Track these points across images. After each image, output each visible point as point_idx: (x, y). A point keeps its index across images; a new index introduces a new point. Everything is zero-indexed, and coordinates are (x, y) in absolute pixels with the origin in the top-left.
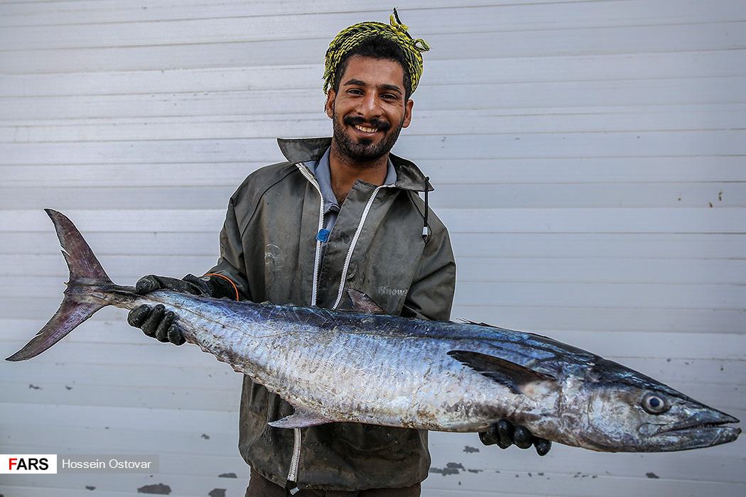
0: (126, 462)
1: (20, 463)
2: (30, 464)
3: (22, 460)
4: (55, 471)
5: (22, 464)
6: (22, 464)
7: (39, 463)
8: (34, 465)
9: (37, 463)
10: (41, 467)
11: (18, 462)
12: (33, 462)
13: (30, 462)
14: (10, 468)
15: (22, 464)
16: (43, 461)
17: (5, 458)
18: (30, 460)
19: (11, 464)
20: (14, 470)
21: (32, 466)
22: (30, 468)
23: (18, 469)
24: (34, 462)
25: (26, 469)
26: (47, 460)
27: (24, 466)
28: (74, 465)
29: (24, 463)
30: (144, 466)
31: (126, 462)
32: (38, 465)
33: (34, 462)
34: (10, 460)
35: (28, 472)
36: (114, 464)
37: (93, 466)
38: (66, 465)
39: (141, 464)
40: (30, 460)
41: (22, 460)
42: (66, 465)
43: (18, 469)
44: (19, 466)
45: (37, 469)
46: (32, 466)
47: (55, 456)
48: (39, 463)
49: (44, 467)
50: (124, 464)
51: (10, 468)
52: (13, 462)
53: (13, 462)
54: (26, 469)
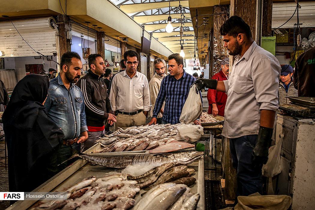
0: (53, 195)
1: (9, 196)
2: (13, 196)
3: (9, 194)
4: (23, 199)
5: (9, 196)
6: (9, 196)
7: (16, 195)
8: (14, 196)
9: (15, 196)
10: (17, 198)
11: (7, 195)
12: (14, 195)
13: (13, 195)
14: (4, 198)
15: (9, 196)
16: (18, 195)
17: (2, 194)
18: (13, 194)
19: (5, 196)
20: (6, 199)
21: (14, 197)
22: (13, 198)
23: (8, 198)
24: (14, 195)
25: (11, 198)
26: (20, 195)
27: (10, 197)
28: (31, 197)
29: (10, 196)
30: (61, 197)
31: (53, 195)
32: (16, 196)
33: (14, 195)
34: (4, 194)
35: (12, 199)
36: (48, 196)
37: (39, 197)
38: (28, 197)
39: (59, 196)
40: (13, 194)
41: (9, 194)
42: (28, 197)
43: (8, 198)
44: (8, 197)
45: (16, 198)
46: (14, 197)
47: (23, 193)
48: (16, 195)
49: (19, 197)
50: (52, 196)
51: (4, 198)
52: (5, 195)
53: (5, 195)
54: (11, 198)
